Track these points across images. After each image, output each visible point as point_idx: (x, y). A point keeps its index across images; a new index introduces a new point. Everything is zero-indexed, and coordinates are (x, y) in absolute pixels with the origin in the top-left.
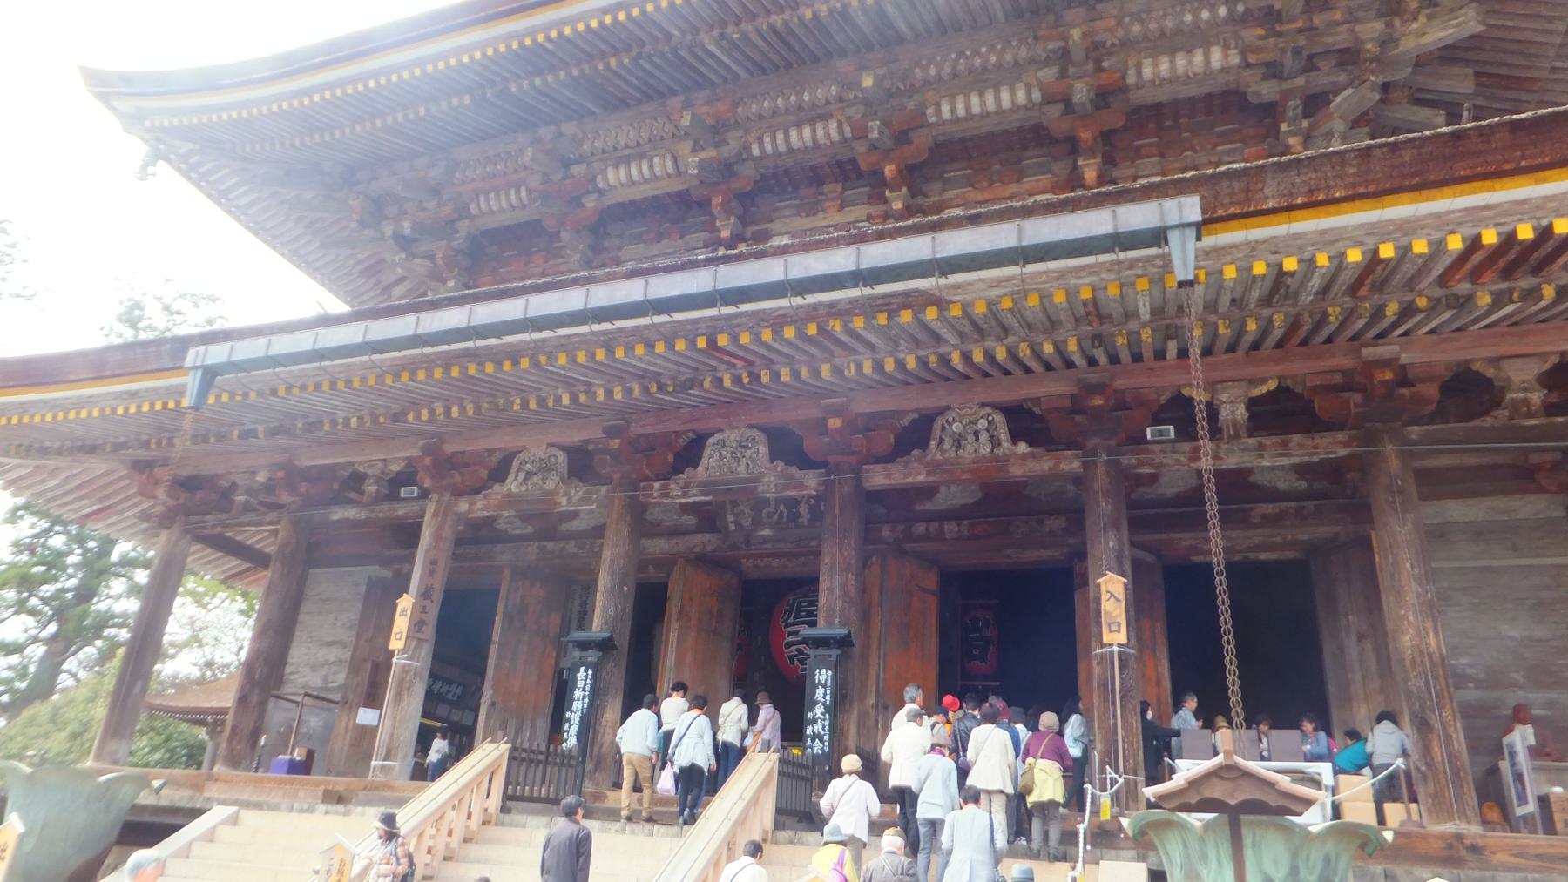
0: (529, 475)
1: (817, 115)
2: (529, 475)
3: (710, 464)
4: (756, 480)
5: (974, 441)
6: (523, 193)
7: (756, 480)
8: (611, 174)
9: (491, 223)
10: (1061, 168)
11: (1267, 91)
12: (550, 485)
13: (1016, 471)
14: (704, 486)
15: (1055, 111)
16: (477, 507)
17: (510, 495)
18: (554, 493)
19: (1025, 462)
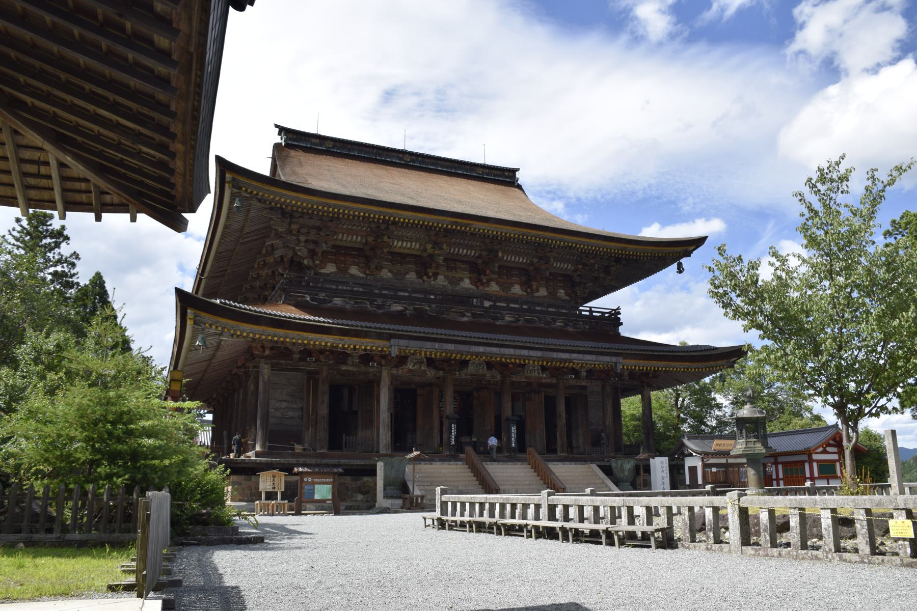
0: (415, 364)
1: (471, 247)
2: (415, 364)
3: (471, 369)
4: (485, 376)
5: (534, 374)
6: (359, 238)
7: (485, 376)
8: (395, 243)
9: (340, 244)
10: (524, 279)
11: (577, 279)
12: (423, 368)
13: (544, 381)
14: (471, 375)
15: (532, 268)
16: (400, 372)
17: (410, 370)
18: (425, 371)
19: (545, 377)
